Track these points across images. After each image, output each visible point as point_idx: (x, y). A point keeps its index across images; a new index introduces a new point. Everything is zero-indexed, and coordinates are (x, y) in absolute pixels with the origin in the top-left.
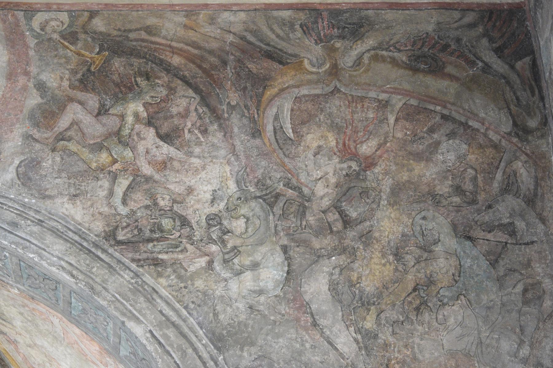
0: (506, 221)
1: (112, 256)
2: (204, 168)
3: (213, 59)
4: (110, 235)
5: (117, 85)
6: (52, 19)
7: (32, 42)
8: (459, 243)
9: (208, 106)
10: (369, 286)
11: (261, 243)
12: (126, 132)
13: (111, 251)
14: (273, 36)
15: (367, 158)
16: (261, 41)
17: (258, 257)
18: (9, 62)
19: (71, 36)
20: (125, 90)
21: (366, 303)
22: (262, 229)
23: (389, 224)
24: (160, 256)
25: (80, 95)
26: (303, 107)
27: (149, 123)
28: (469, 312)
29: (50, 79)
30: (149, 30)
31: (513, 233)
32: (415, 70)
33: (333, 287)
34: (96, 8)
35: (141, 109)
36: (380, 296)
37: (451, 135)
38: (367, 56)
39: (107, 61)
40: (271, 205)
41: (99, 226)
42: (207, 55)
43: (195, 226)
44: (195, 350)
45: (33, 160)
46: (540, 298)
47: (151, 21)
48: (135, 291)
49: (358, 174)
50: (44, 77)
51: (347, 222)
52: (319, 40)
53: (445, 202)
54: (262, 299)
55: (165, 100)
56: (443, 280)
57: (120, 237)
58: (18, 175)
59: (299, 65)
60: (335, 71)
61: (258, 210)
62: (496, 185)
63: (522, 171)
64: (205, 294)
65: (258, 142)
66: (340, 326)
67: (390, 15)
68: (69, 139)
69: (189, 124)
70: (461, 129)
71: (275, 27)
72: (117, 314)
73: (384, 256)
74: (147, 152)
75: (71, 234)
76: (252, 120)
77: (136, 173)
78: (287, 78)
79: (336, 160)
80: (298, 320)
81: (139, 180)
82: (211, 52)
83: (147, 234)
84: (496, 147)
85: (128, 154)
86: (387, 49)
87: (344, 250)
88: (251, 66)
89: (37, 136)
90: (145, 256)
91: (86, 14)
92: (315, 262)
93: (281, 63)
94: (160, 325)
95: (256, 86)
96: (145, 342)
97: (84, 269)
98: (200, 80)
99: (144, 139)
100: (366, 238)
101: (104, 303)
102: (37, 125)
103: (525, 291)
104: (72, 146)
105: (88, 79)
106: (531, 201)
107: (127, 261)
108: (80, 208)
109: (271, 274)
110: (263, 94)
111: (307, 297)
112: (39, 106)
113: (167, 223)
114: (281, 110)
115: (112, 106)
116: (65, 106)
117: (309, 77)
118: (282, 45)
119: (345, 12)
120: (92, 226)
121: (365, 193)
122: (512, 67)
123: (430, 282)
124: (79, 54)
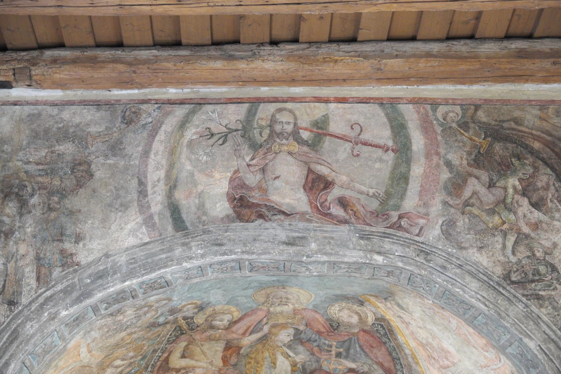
1: (509, 292)
4: (507, 277)
5: (499, 164)
6: (450, 111)
7: (439, 130)
12: (509, 200)
13: (508, 288)
19: (464, 126)
24: (541, 293)
25: (476, 171)
29: (454, 157)
35: (517, 183)
39: (491, 145)
41: (499, 270)
45: (450, 221)
50: (450, 157)
57: (513, 279)
58: (442, 231)
68: (472, 205)
72: (517, 333)
74: (525, 216)
75: (481, 276)
77: (519, 232)
81: (521, 238)
83: (531, 277)
85: (512, 217)
89: (451, 203)
90: (530, 292)
96: (536, 352)
97: (492, 301)
99: (522, 206)
101: (508, 325)
102: (450, 194)
104: (475, 211)
105: (480, 159)
107: (520, 296)
108: (485, 256)
112: (450, 179)
113: (542, 269)
115: (498, 181)
116: (467, 180)
120: (495, 270)
124: (471, 139)
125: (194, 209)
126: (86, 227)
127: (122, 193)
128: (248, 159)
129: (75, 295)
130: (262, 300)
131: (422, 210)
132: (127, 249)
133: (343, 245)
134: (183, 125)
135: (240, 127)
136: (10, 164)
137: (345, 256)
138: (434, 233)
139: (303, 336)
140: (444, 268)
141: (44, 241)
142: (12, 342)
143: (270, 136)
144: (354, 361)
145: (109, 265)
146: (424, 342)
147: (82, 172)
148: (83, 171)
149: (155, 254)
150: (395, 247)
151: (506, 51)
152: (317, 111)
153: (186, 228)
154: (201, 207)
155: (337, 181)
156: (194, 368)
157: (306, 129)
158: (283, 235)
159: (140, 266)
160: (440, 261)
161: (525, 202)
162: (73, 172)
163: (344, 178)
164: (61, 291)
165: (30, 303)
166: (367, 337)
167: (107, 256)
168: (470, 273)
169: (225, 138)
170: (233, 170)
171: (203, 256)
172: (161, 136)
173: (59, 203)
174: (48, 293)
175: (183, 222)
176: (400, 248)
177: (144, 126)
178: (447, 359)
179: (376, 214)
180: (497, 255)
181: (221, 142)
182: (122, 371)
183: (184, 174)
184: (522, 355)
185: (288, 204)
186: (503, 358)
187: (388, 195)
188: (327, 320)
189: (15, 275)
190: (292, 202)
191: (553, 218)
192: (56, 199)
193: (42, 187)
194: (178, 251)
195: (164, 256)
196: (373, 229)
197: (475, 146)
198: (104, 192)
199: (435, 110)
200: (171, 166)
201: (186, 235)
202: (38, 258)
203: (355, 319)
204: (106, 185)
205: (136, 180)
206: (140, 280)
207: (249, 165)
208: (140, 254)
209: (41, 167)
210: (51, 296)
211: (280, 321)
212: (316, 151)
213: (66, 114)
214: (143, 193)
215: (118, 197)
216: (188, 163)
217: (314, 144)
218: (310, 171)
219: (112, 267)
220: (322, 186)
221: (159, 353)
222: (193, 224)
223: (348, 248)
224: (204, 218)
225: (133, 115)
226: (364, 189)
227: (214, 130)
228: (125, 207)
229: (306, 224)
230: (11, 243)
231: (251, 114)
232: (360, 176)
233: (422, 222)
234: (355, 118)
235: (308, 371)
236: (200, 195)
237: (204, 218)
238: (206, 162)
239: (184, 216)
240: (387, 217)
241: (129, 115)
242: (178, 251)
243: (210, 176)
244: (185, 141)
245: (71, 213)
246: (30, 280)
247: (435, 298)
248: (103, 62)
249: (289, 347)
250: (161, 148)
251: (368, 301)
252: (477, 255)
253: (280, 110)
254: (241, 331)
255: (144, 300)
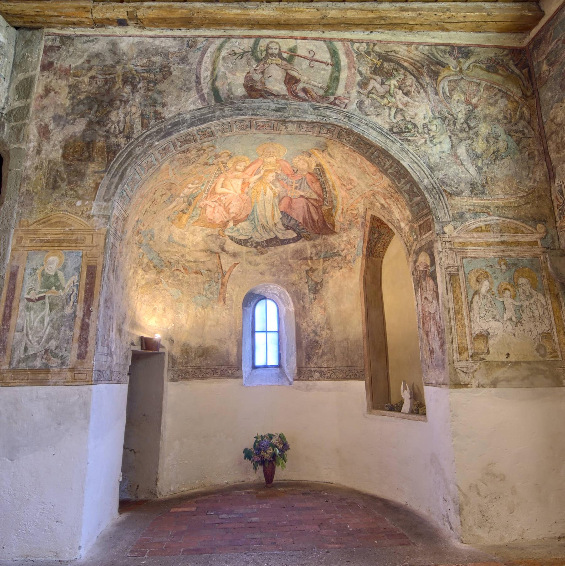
0: (521, 129)
2: (420, 106)
3: (418, 64)
4: (391, 130)
5: (387, 73)
7: (355, 55)
8: (507, 137)
9: (419, 82)
10: (479, 151)
11: (442, 135)
12: (392, 91)
14: (439, 56)
15: (475, 104)
16: (435, 58)
17: (441, 140)
18: (348, 63)
19: (368, 53)
20: (389, 75)
21: (478, 157)
22: (442, 130)
23: (484, 129)
24: (409, 138)
25: (375, 77)
26: (452, 84)
27: (400, 88)
28: (511, 161)
29: (363, 69)
30: (395, 52)
31: (524, 134)
32: (489, 72)
33: (467, 151)
34: (376, 42)
35: (396, 83)
36: (482, 155)
37: (502, 97)
38: (471, 65)
39: (382, 63)
40: (444, 121)
41: (387, 127)
42: (416, 63)
43: (418, 126)
44: (424, 171)
45: (362, 101)
46: (534, 157)
47: (395, 48)
48: (402, 150)
49: (472, 110)
50: (360, 69)
51: (470, 128)
52: (455, 59)
53: (501, 122)
54: (444, 154)
55: (404, 80)
56: (502, 150)
57: (395, 131)
59: (449, 68)
60: (461, 71)
61: (439, 122)
62: (517, 116)
63: (526, 111)
64: (425, 152)
65: (437, 97)
66: (470, 165)
67: (478, 49)
68: (373, 94)
69: (413, 89)
70: (506, 95)
71: (440, 53)
73: (483, 141)
76: (435, 89)
78: (444, 73)
79: (464, 105)
80: (456, 162)
81: (399, 110)
82: (418, 61)
83: (404, 130)
84: (517, 102)
85: (393, 100)
86: (478, 63)
87: (469, 138)
88: (432, 67)
89: (362, 92)
90: (403, 138)
91: (372, 44)
92: (460, 142)
93: (444, 67)
94: (411, 162)
95: (435, 75)
98: (415, 73)
100: (476, 134)
102: (361, 87)
103: (529, 154)
104: (374, 97)
105: (376, 70)
106: (529, 123)
107: (398, 140)
109: (446, 146)
110: (437, 79)
111: (459, 154)
112: (361, 80)
113: (410, 126)
114: (444, 85)
117: (453, 73)
118: (442, 60)
119: (463, 47)
120: (385, 126)
121: (475, 117)
122: (521, 72)
123: (498, 150)
125: (226, 91)
126: (168, 100)
127: (187, 82)
128: (254, 66)
129: (162, 134)
130: (261, 153)
131: (347, 96)
132: (190, 111)
133: (305, 112)
134: (219, 49)
135: (250, 50)
136: (127, 66)
137: (306, 118)
138: (353, 107)
139: (279, 177)
140: (359, 125)
141: (145, 106)
142: (128, 158)
143: (267, 55)
144: (303, 191)
145: (181, 119)
146: (340, 176)
147: (166, 72)
148: (166, 71)
149: (205, 114)
150: (332, 114)
151: (393, 8)
152: (291, 43)
153: (222, 101)
154: (230, 90)
155: (302, 80)
156: (228, 193)
157: (285, 52)
158: (273, 106)
159: (197, 120)
160: (356, 122)
161: (400, 92)
162: (161, 72)
163: (305, 78)
164: (155, 132)
165: (138, 138)
166: (311, 177)
167: (180, 114)
168: (372, 128)
169: (242, 56)
170: (246, 72)
171: (231, 116)
172: (208, 54)
173: (152, 87)
174: (148, 133)
175: (220, 98)
176: (335, 114)
177: (199, 49)
178: (351, 184)
179: (322, 97)
180: (386, 119)
181: (240, 57)
182: (193, 191)
183: (220, 74)
184: (397, 172)
185: (276, 91)
186: (384, 176)
187: (329, 87)
188: (292, 167)
189: (130, 123)
190: (278, 89)
191: (415, 101)
192: (152, 85)
193: (144, 78)
194: (218, 113)
195: (210, 115)
196: (321, 105)
197: (374, 64)
198: (178, 82)
199: (352, 45)
200: (214, 69)
201: (222, 105)
202: (142, 115)
203: (305, 167)
204: (179, 78)
205: (195, 76)
206: (198, 128)
207: (255, 70)
208: (197, 114)
209: (143, 68)
210: (150, 134)
211: (270, 168)
212: (291, 64)
213: (157, 42)
214: (198, 82)
215: (185, 85)
216: (222, 68)
217: (290, 60)
218: (287, 74)
219: (182, 120)
220: (294, 82)
221: (210, 184)
222: (225, 99)
223: (308, 113)
224: (232, 96)
225: (193, 43)
226: (316, 84)
227: (236, 51)
228: (189, 89)
229: (286, 101)
230: (128, 107)
231: (256, 44)
232: (315, 78)
233: (346, 101)
234: (310, 47)
235: (281, 197)
236: (229, 84)
237: (232, 96)
238: (232, 68)
239: (221, 95)
240: (329, 99)
241: (192, 44)
242: (218, 113)
243: (234, 75)
244: (221, 57)
245: (160, 92)
246: (138, 126)
247: (351, 145)
248: (176, 9)
249: (273, 183)
250: (208, 60)
251: (314, 153)
252: (376, 118)
253: (271, 42)
254: (250, 173)
255: (201, 144)
